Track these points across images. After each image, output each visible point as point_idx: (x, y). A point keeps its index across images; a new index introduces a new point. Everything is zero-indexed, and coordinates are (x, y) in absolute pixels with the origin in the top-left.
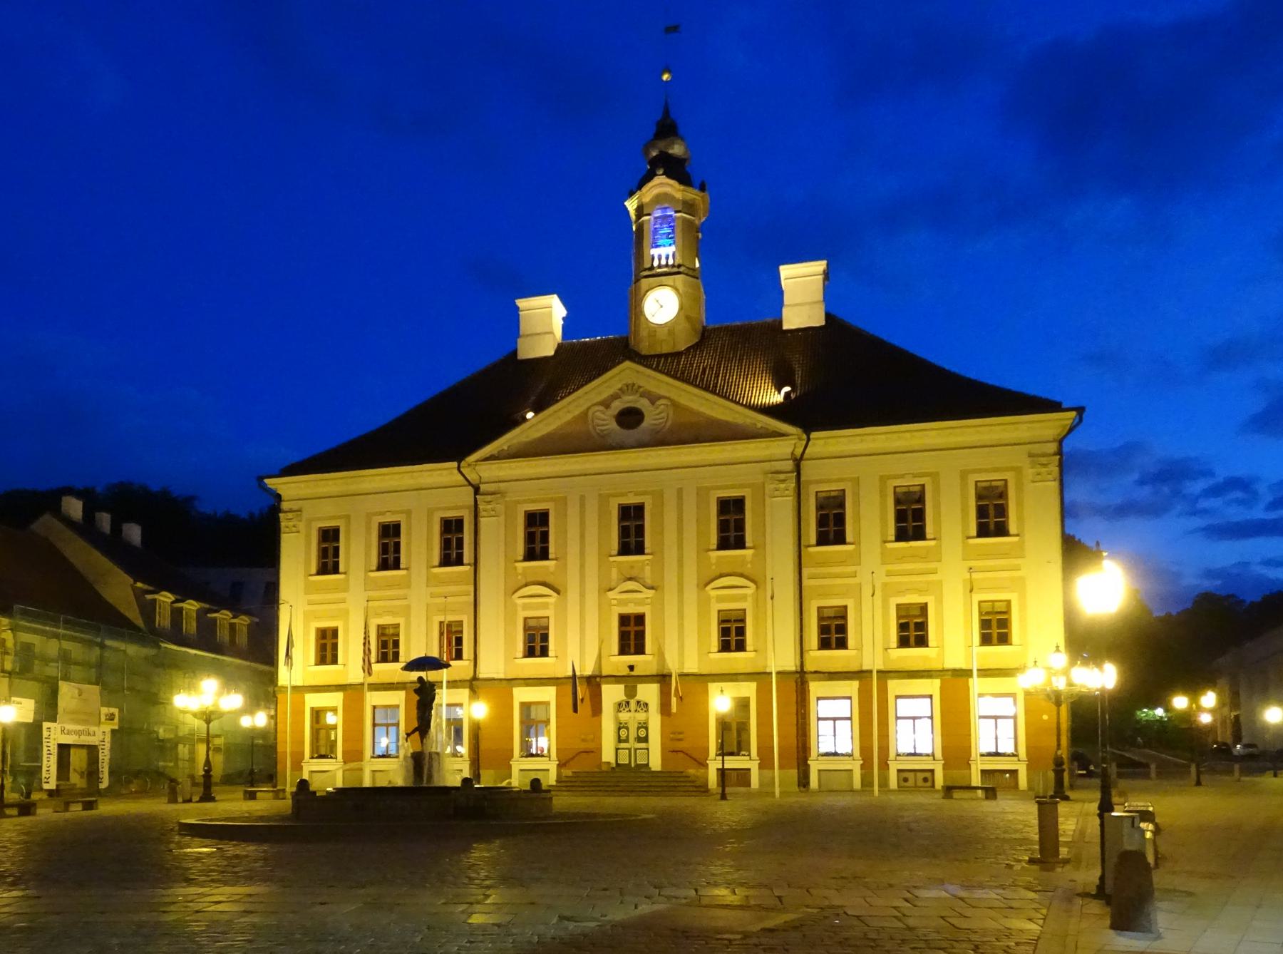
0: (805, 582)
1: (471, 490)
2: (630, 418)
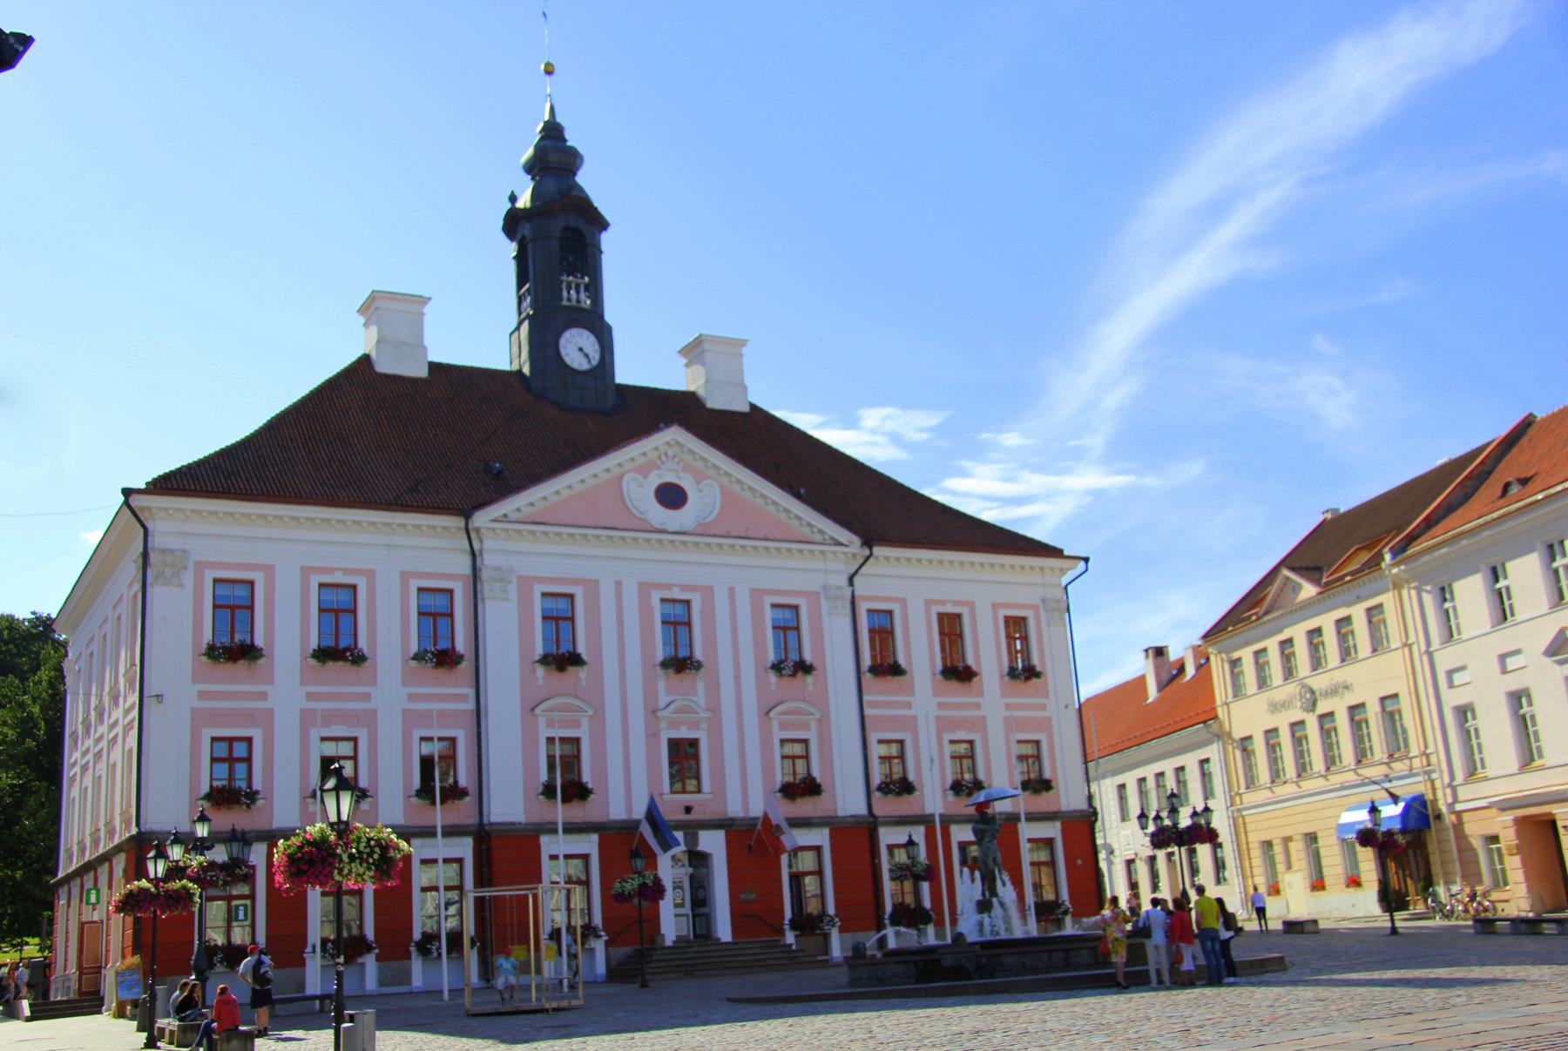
0: (867, 711)
1: (467, 560)
2: (671, 496)
